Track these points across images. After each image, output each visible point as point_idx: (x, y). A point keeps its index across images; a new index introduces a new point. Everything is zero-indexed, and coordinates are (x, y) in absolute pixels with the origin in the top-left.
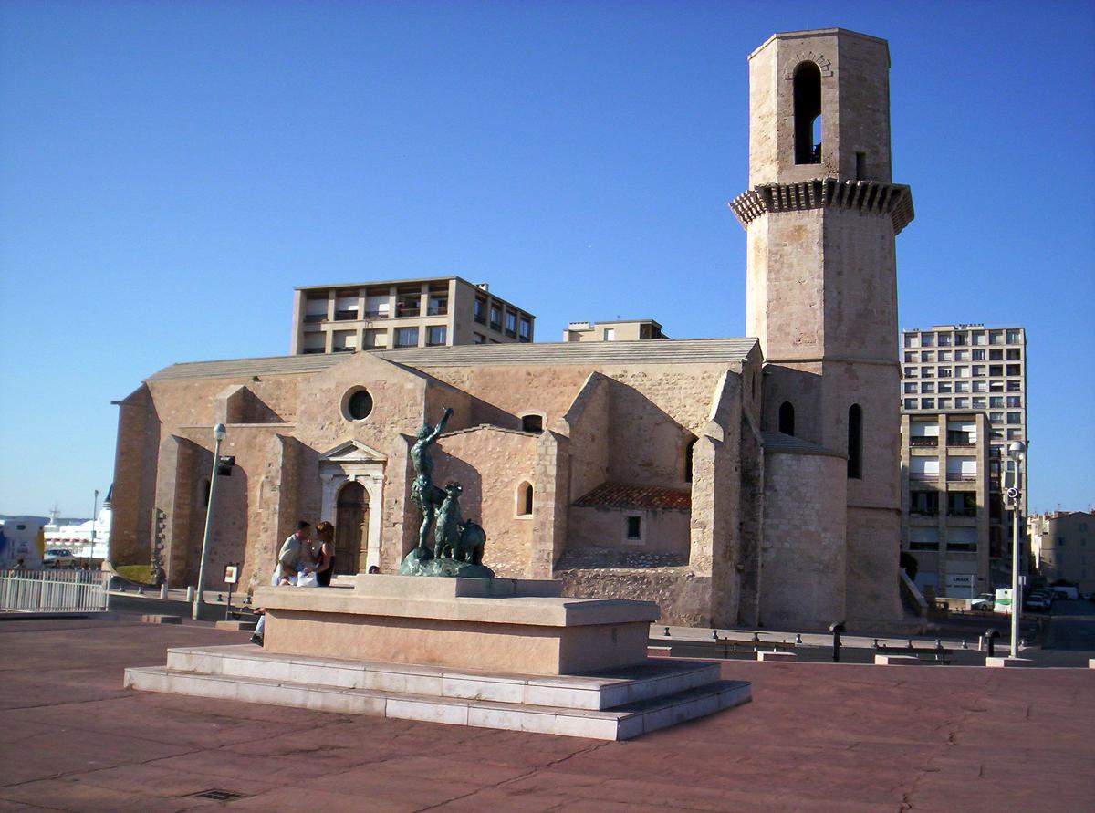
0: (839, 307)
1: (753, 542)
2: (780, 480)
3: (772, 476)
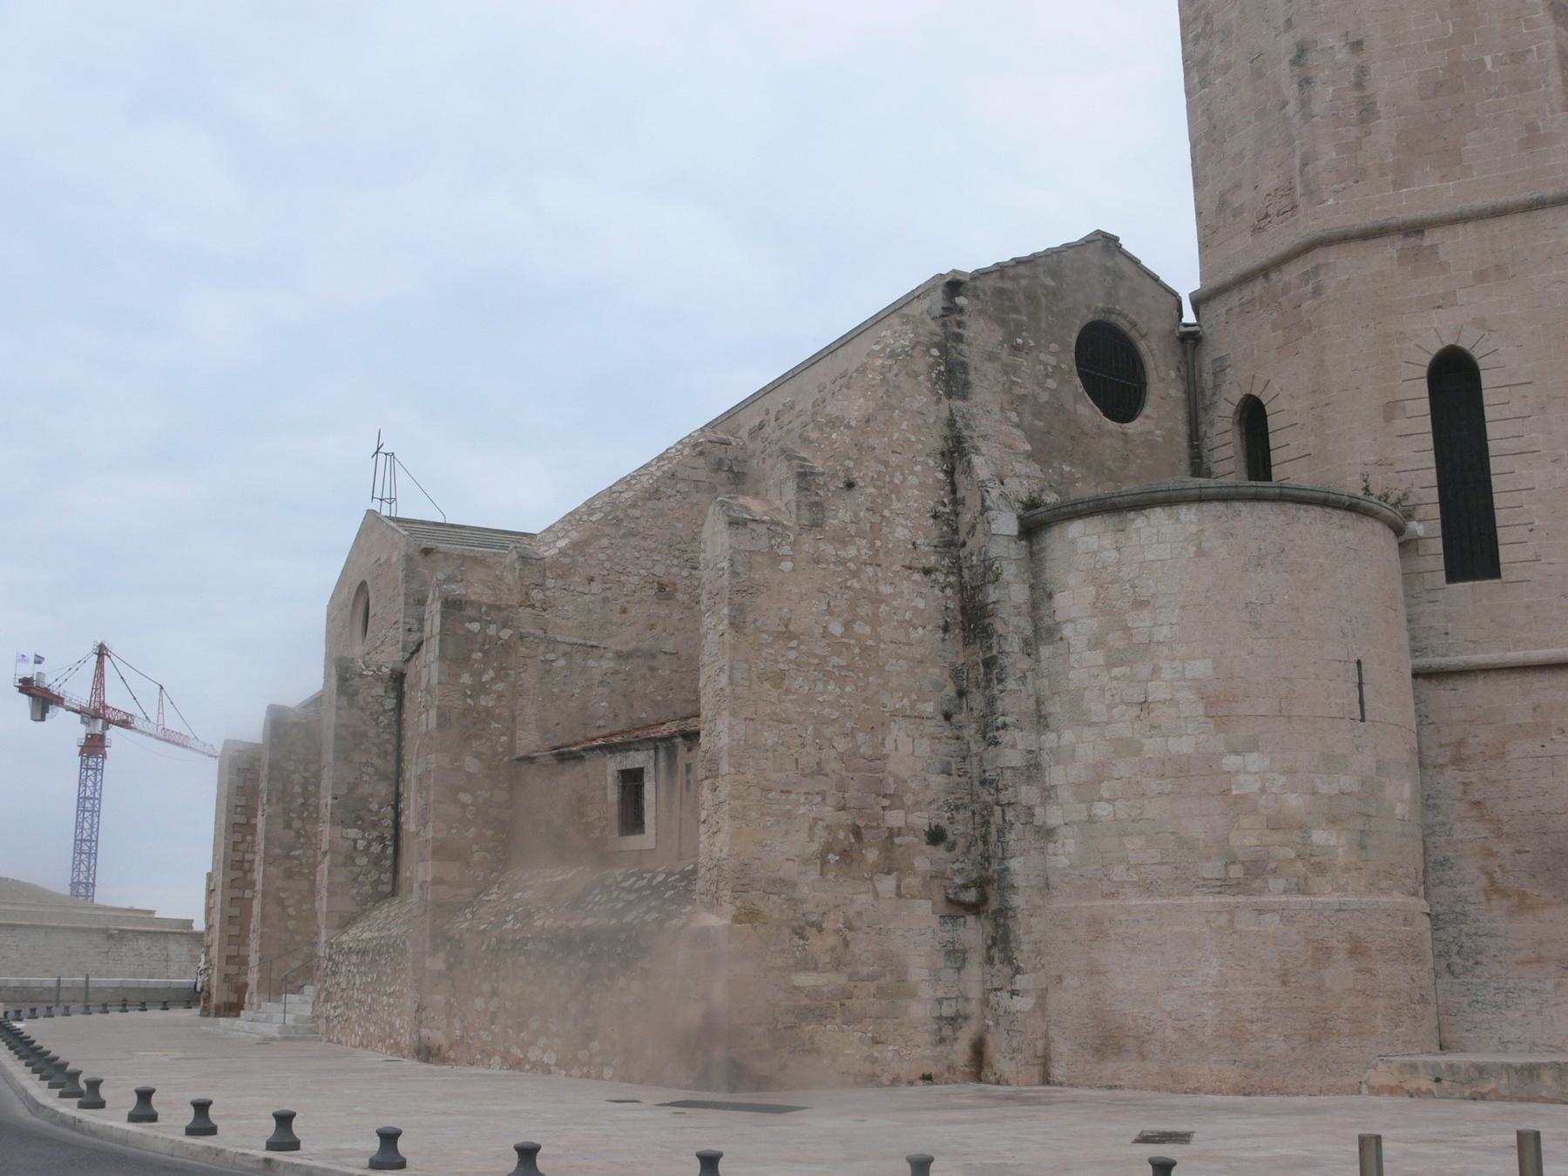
0: (1359, 86)
1: (998, 809)
2: (1072, 602)
3: (1050, 596)
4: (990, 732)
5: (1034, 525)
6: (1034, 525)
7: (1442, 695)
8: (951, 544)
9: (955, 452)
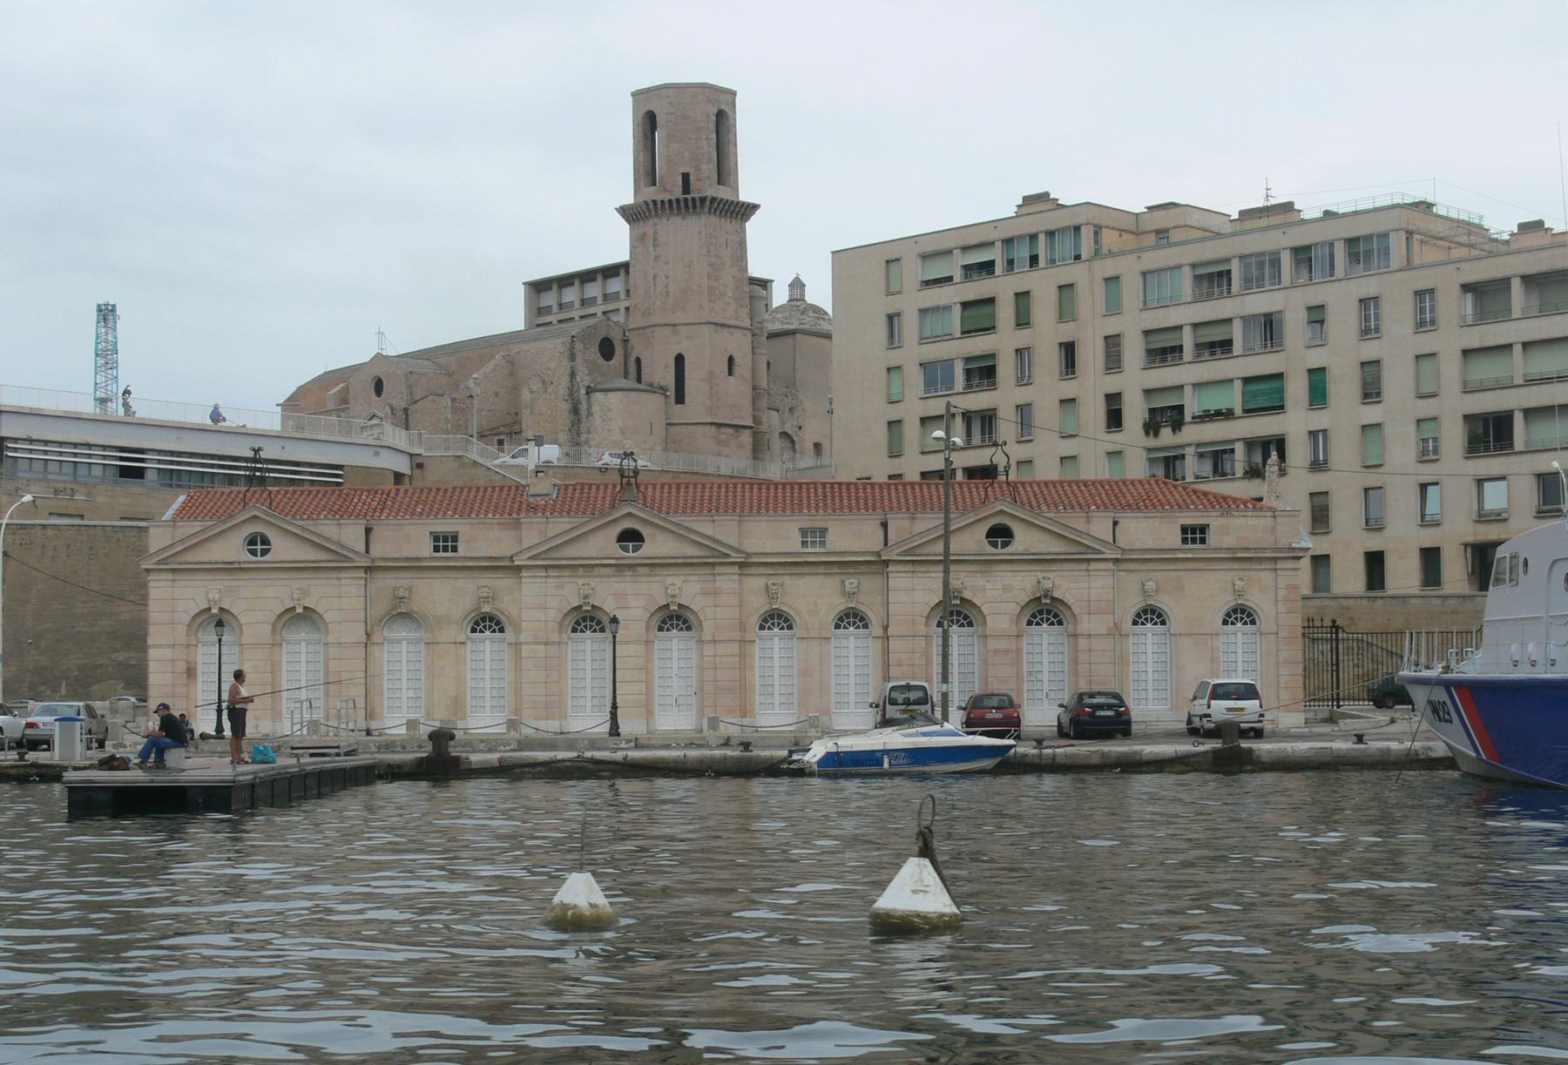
2: (596, 409)
4: (578, 434)
5: (590, 391)
6: (590, 391)
7: (671, 428)
8: (571, 394)
9: (573, 374)
